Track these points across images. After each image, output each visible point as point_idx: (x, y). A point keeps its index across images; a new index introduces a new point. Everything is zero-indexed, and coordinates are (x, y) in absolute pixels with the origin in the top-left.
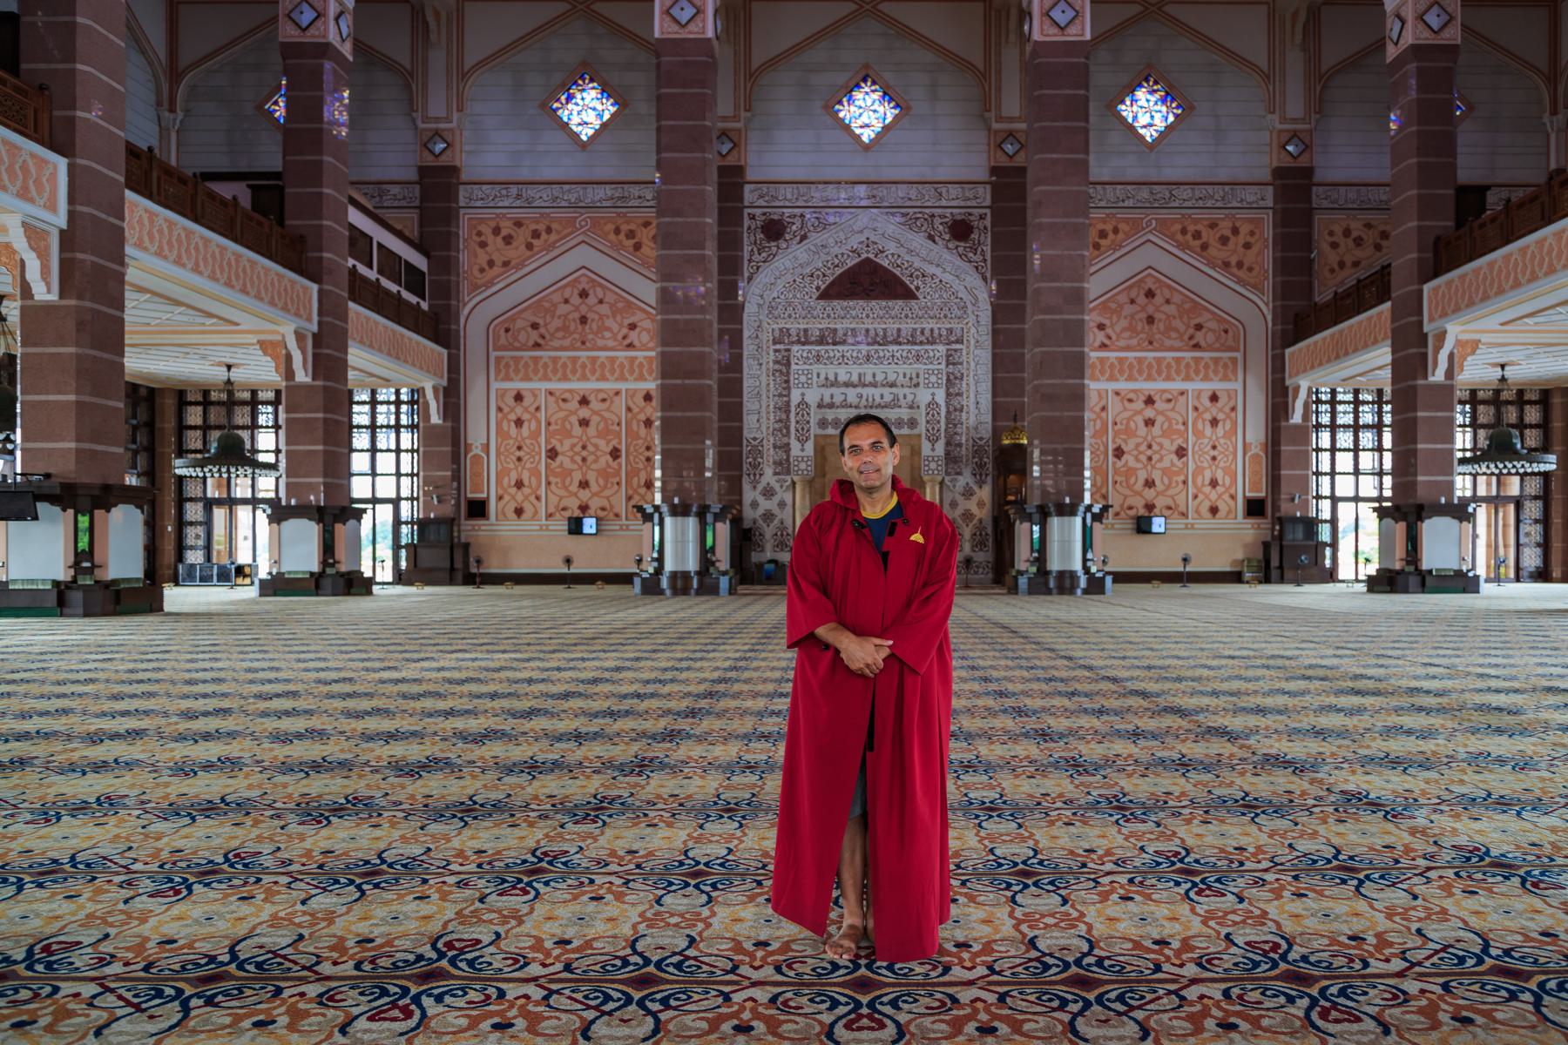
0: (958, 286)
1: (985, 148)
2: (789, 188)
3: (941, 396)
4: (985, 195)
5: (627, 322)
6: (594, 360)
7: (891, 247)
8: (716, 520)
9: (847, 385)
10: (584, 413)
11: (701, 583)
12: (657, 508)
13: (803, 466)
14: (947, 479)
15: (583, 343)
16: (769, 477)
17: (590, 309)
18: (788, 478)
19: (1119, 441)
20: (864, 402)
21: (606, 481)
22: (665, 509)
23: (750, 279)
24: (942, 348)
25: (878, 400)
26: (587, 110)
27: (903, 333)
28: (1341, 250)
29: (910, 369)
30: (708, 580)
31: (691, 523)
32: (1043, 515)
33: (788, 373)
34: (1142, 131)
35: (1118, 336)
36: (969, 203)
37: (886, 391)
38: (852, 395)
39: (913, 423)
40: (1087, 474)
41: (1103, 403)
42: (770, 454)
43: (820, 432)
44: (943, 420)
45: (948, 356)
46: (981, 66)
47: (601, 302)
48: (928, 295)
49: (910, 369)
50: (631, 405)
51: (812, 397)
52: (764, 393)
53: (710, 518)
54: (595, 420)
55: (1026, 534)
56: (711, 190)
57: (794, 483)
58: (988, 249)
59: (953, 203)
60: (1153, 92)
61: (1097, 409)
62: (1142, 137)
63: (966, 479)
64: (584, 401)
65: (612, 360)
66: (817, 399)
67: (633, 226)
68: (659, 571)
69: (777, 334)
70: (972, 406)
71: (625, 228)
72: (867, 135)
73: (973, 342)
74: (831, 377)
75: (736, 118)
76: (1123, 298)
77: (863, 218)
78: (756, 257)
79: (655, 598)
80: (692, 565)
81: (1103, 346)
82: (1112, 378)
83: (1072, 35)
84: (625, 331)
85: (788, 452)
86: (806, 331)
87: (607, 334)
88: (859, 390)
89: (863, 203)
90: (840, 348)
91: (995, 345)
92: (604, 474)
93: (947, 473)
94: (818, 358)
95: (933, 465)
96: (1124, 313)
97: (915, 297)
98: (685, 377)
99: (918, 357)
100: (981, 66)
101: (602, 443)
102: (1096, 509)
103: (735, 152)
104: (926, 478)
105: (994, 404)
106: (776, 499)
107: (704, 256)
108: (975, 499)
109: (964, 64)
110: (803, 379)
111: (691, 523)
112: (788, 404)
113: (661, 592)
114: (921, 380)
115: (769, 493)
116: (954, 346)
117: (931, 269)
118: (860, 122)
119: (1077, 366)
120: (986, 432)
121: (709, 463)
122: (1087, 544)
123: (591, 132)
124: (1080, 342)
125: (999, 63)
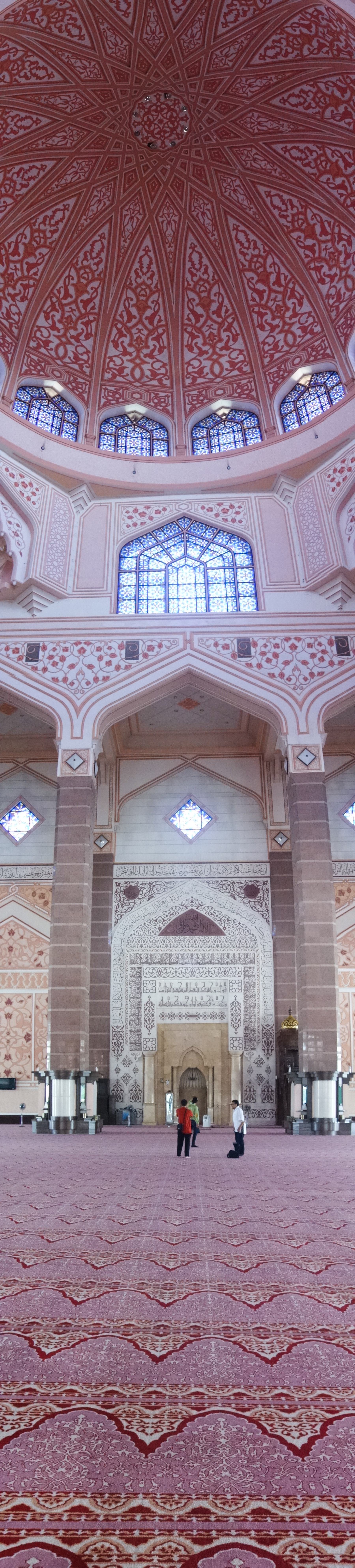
0: (250, 927)
1: (265, 840)
2: (142, 867)
3: (240, 998)
5: (37, 950)
6: (15, 975)
7: (207, 903)
8: (87, 1082)
9: (178, 990)
10: (9, 1009)
12: (47, 1073)
13: (149, 1044)
14: (245, 1052)
15: (10, 964)
17: (15, 942)
18: (140, 1052)
20: (190, 1002)
21: (22, 1056)
22: (52, 1074)
23: (116, 923)
25: (199, 1000)
26: (21, 822)
27: (216, 957)
29: (220, 980)
30: (80, 1124)
31: (70, 1083)
32: (311, 1078)
37: (205, 994)
38: (182, 997)
39: (222, 1015)
44: (242, 1014)
46: (260, 793)
47: (22, 937)
49: (220, 980)
50: (38, 1005)
51: (156, 998)
52: (124, 996)
53: (83, 1080)
54: (15, 1014)
57: (143, 1056)
58: (269, 903)
63: (259, 1053)
64: (9, 1002)
65: (27, 975)
67: (43, 891)
68: (48, 1116)
69: (133, 957)
70: (262, 1004)
71: (38, 892)
72: (191, 835)
73: (261, 962)
74: (168, 986)
77: (189, 885)
80: (70, 1113)
83: (314, 769)
84: (36, 955)
85: (140, 1035)
86: (151, 955)
87: (25, 958)
88: (187, 994)
90: (174, 966)
91: (275, 965)
92: (20, 1050)
93: (246, 1049)
94: (160, 973)
95: (236, 1044)
97: (223, 934)
98: (67, 985)
99: (225, 972)
100: (260, 793)
103: (108, 846)
104: (231, 1052)
105: (276, 1002)
106: (132, 1067)
108: (264, 1066)
109: (248, 792)
110: (150, 987)
111: (70, 1083)
112: (140, 1003)
114: (228, 987)
115: (126, 1063)
116: (249, 965)
120: (271, 1021)
121: (82, 1043)
125: (270, 791)
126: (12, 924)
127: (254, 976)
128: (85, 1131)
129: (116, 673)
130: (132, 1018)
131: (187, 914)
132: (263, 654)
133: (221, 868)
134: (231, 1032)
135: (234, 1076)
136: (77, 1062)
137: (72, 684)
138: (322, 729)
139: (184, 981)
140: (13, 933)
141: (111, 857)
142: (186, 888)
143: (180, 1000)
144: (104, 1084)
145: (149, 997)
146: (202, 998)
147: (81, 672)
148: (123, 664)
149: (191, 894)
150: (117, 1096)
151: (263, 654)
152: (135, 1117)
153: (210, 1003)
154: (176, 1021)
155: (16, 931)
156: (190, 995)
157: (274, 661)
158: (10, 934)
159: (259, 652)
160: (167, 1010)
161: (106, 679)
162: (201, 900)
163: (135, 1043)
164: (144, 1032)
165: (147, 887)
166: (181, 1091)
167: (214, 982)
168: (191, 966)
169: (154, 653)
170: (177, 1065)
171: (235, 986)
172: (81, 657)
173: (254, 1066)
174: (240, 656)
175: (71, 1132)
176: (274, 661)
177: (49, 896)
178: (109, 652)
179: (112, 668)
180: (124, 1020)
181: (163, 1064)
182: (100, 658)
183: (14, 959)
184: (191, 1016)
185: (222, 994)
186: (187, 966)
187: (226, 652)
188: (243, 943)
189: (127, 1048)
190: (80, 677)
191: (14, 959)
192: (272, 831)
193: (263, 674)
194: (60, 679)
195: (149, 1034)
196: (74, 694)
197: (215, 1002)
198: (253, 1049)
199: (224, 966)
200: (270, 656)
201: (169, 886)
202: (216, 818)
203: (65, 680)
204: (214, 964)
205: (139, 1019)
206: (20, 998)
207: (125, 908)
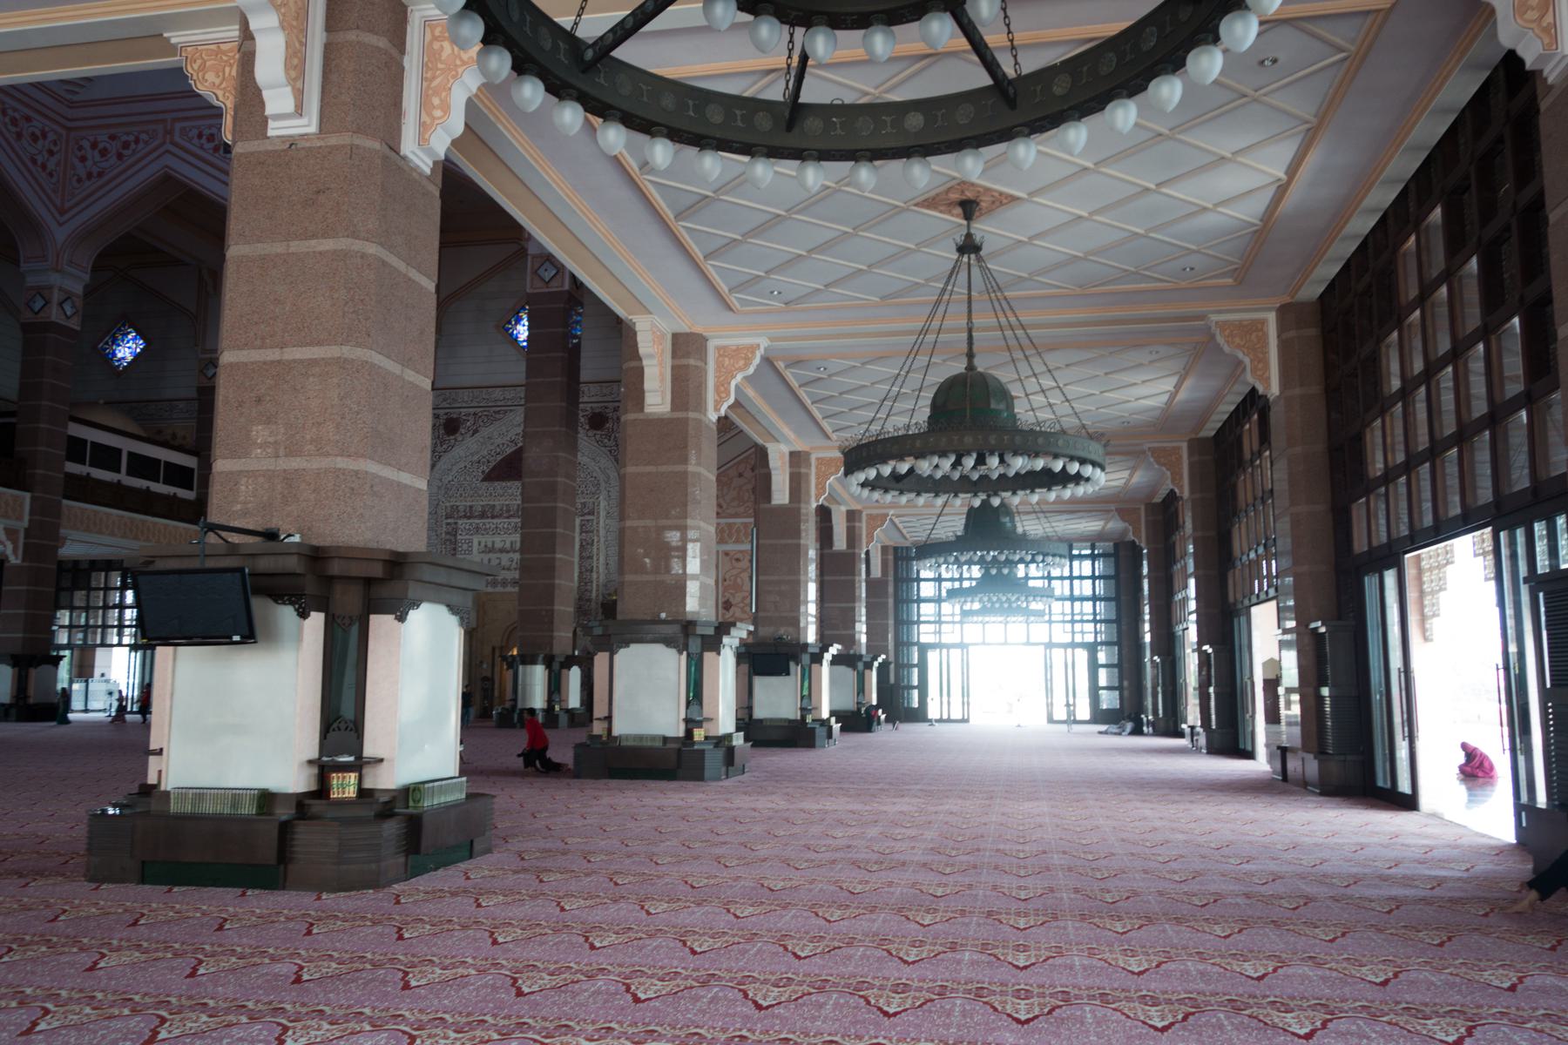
9: (502, 551)
28: (89, 163)
154: (499, 589)
165: (471, 419)
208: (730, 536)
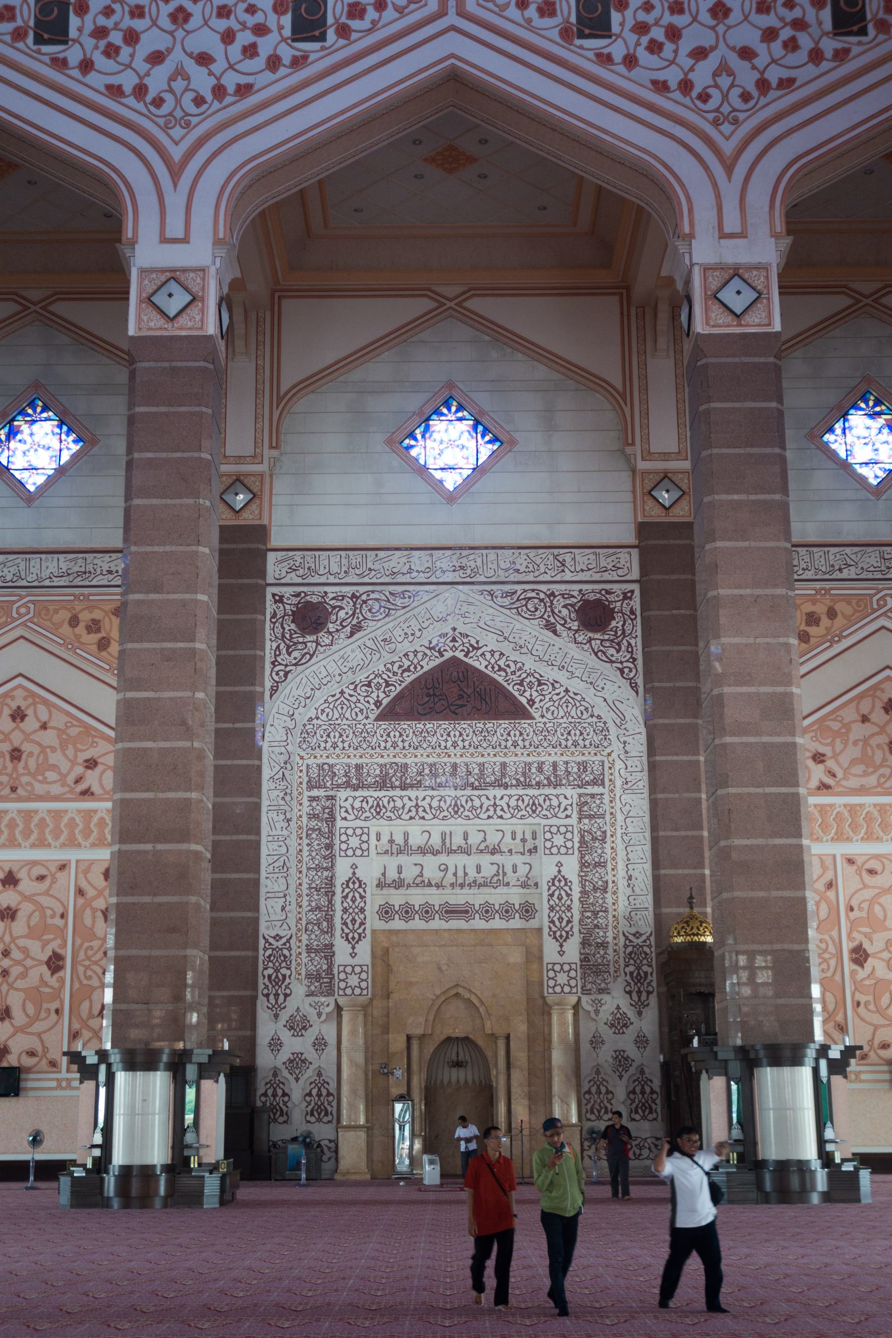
0: (595, 700)
1: (629, 497)
2: (335, 557)
3: (571, 867)
4: (630, 564)
5: (82, 757)
6: (28, 815)
7: (490, 642)
8: (201, 1077)
9: (423, 851)
11: (170, 1184)
12: (103, 1055)
13: (353, 980)
14: (584, 999)
15: (14, 789)
16: (299, 997)
17: (27, 737)
18: (331, 1000)
19: (859, 937)
20: (450, 878)
22: (115, 1058)
23: (274, 690)
24: (569, 792)
25: (472, 873)
26: (39, 448)
27: (511, 770)
29: (521, 826)
30: (184, 1181)
31: (159, 1082)
32: (746, 1064)
33: (331, 832)
34: (864, 471)
35: (846, 771)
36: (606, 576)
37: (485, 860)
38: (431, 866)
39: (528, 911)
40: (816, 990)
41: (829, 875)
42: (303, 962)
43: (381, 925)
45: (581, 805)
47: (44, 726)
48: (544, 711)
49: (521, 826)
50: (84, 885)
51: (370, 870)
52: (293, 863)
53: (191, 1071)
55: (716, 1096)
56: (207, 552)
57: (339, 1009)
59: (581, 576)
60: (874, 416)
61: (820, 886)
62: (862, 479)
63: (616, 1000)
64: (11, 880)
65: (57, 815)
66: (377, 873)
67: (97, 615)
68: (102, 1164)
70: (622, 883)
71: (85, 617)
73: (619, 783)
74: (399, 839)
75: (256, 458)
76: (850, 714)
78: (284, 658)
79: (96, 1211)
80: (157, 1154)
81: (824, 787)
82: (839, 837)
83: (753, 324)
84: (79, 770)
86: (358, 767)
87: (51, 776)
88: (443, 858)
89: (450, 577)
90: (412, 793)
93: (586, 991)
94: (378, 809)
95: (562, 978)
96: (852, 737)
97: (528, 716)
99: (534, 807)
101: (34, 946)
102: (835, 1053)
103: (254, 507)
104: (550, 999)
105: (657, 880)
106: (310, 1035)
107: (193, 651)
108: (631, 1033)
110: (354, 842)
111: (159, 1082)
113: (105, 1203)
114: (539, 842)
115: (299, 1026)
116: (590, 790)
117: (550, 674)
118: (440, 463)
119: (788, 817)
120: (646, 924)
122: (823, 1114)
123: (40, 479)
124: (791, 777)
126: (20, 693)
127: (602, 816)
128: (194, 1198)
129: (268, 76)
130: (312, 916)
131: (441, 667)
132: (641, 28)
133: (522, 561)
134: (550, 949)
135: (558, 1057)
136: (178, 1028)
137: (158, 102)
138: (780, 227)
139: (437, 829)
140: (23, 717)
141: (261, 532)
142: (438, 608)
143: (427, 874)
144: (241, 1077)
145: (354, 867)
146: (479, 869)
147: (180, 73)
148: (286, 53)
149: (451, 623)
150: (273, 1109)
151: (641, 28)
152: (318, 1160)
153: (498, 880)
154: (417, 924)
155: (30, 712)
156: (453, 861)
157: (669, 47)
158: (13, 717)
159: (630, 23)
160: (397, 898)
161: (244, 90)
162: (477, 635)
163: (318, 977)
164: (342, 949)
165: (348, 605)
166: (430, 1095)
167: (508, 830)
168: (453, 793)
169: (365, 24)
170: (419, 1031)
171: (559, 840)
172: (180, 34)
173: (606, 1032)
174: (582, 35)
175: (158, 1203)
176: (669, 47)
177: (112, 627)
178: (251, 20)
179: (259, 63)
180: (292, 922)
181: (386, 1029)
182: (228, 37)
183: (25, 779)
184: (451, 912)
185: (527, 858)
186: (443, 792)
187: (547, 22)
188: (575, 736)
189: (299, 989)
190: (179, 85)
191: (25, 779)
192: (645, 473)
193: (637, 81)
194: (128, 89)
195: (353, 955)
196: (165, 129)
197: (511, 877)
198: (601, 991)
199: (531, 792)
200: (658, 33)
201: (399, 602)
202: (513, 442)
203: (140, 91)
204: (506, 787)
205: (330, 920)
206: (38, 871)
207: (296, 654)
208: (854, 827)
